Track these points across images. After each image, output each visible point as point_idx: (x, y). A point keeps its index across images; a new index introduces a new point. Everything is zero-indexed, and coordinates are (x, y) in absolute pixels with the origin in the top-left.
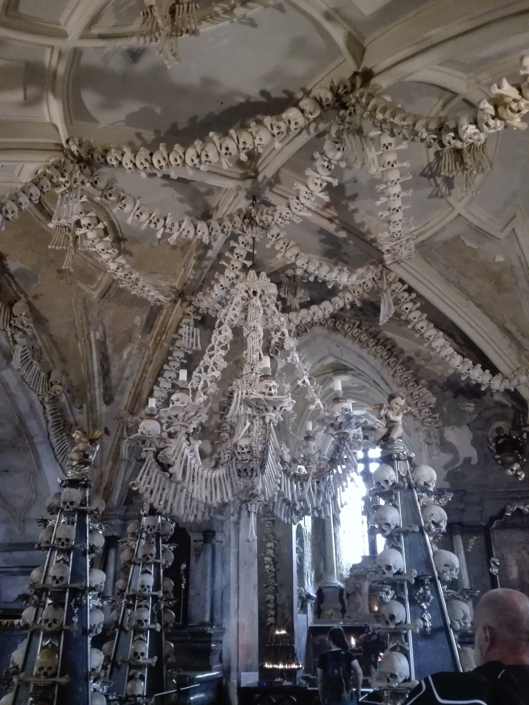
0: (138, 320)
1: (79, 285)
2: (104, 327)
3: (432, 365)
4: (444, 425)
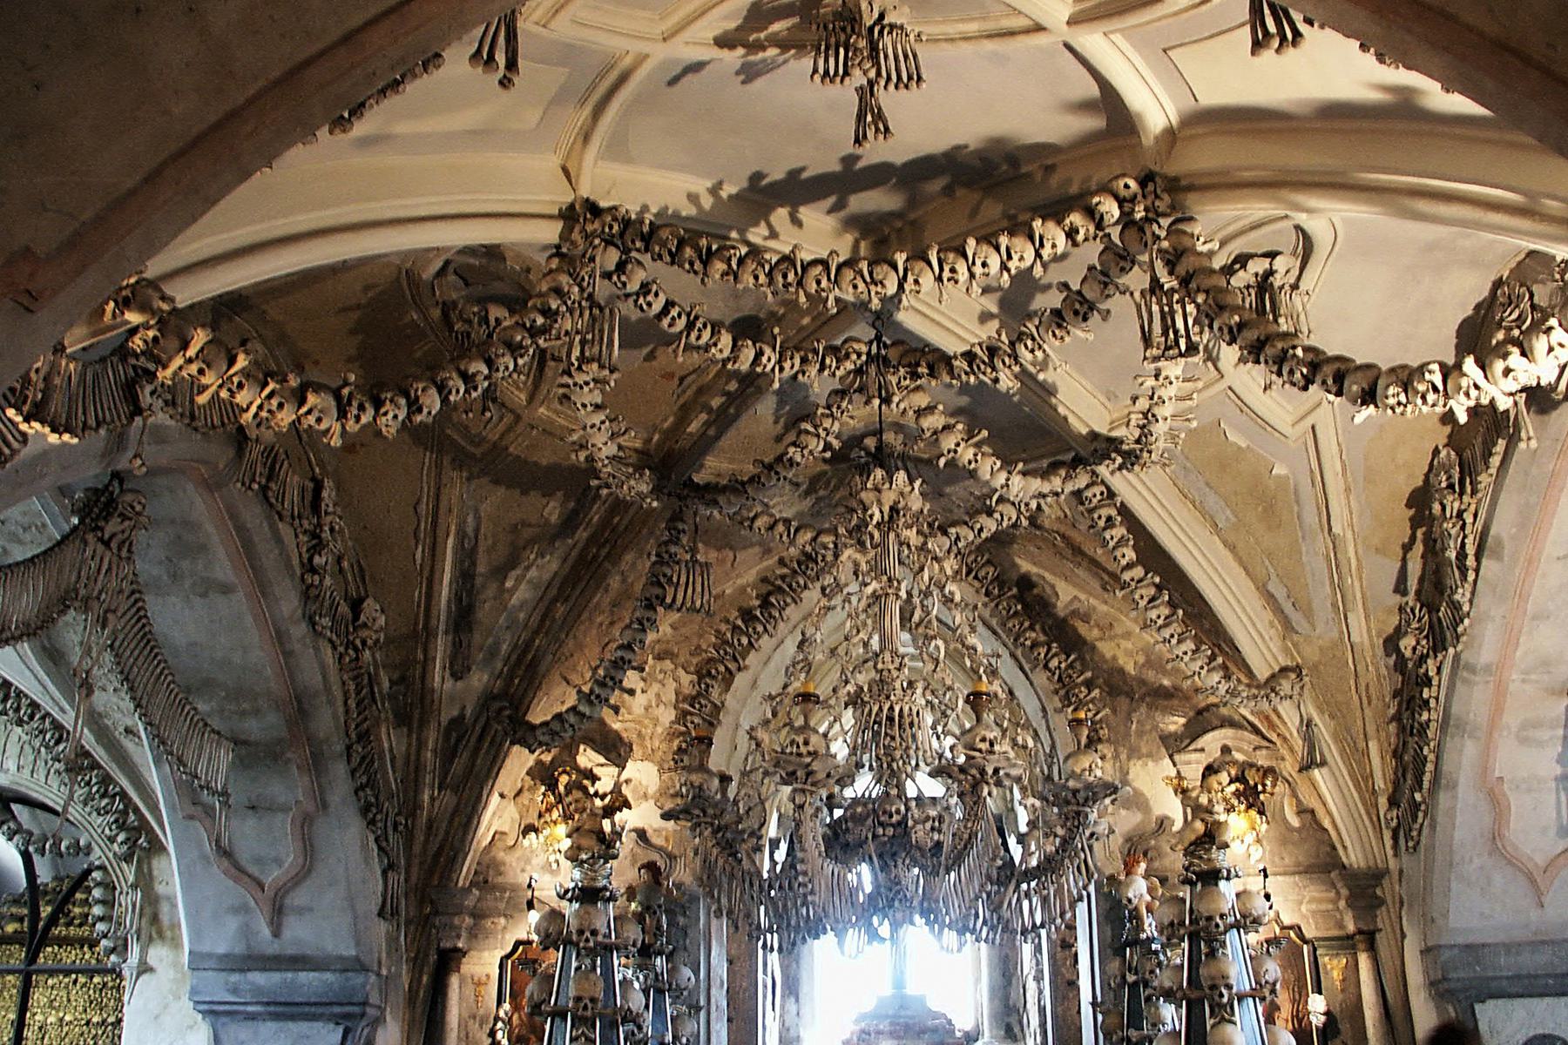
0: (553, 511)
1: (449, 431)
2: (478, 519)
3: (1112, 638)
4: (1129, 758)
